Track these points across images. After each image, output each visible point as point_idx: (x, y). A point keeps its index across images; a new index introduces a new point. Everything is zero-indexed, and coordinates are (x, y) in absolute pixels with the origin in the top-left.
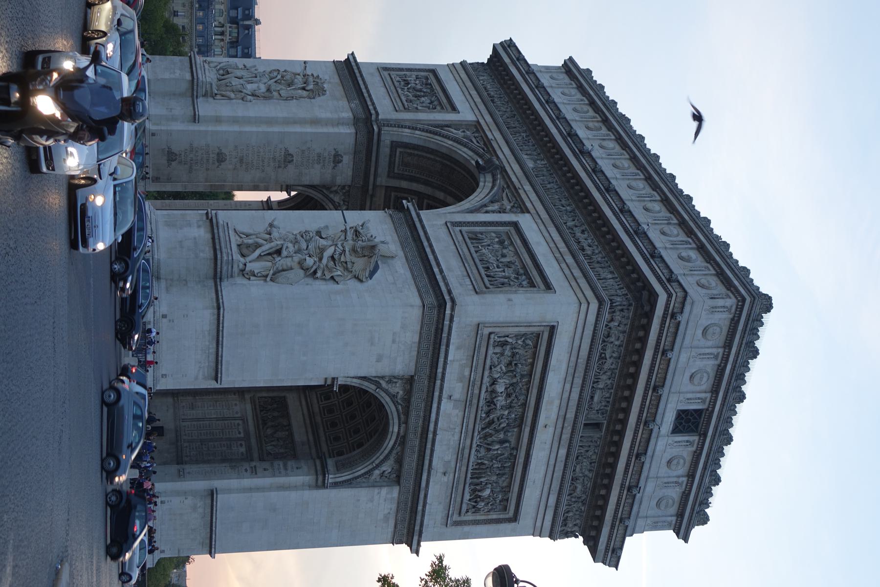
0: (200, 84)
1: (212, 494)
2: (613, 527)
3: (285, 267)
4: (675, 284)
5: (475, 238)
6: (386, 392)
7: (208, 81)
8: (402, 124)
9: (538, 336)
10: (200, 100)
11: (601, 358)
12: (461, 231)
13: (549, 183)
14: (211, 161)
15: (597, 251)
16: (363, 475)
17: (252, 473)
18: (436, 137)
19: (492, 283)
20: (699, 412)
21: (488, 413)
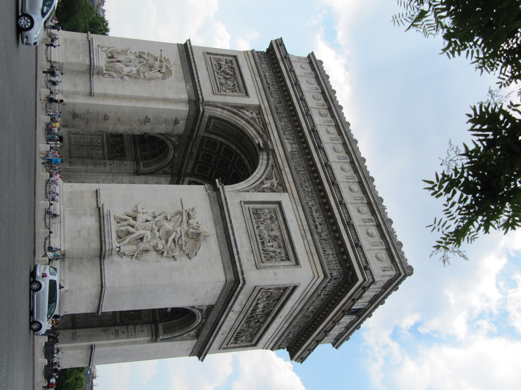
0: (95, 67)
1: (92, 348)
2: (304, 351)
3: (145, 249)
4: (368, 271)
5: (256, 213)
6: (198, 309)
7: (100, 66)
8: (217, 104)
9: (287, 288)
10: (95, 77)
11: (318, 295)
12: (249, 208)
13: (299, 166)
14: (100, 119)
15: (324, 230)
16: (178, 336)
17: (116, 335)
18: (236, 117)
19: (265, 255)
20: (360, 309)
21: (251, 314)
